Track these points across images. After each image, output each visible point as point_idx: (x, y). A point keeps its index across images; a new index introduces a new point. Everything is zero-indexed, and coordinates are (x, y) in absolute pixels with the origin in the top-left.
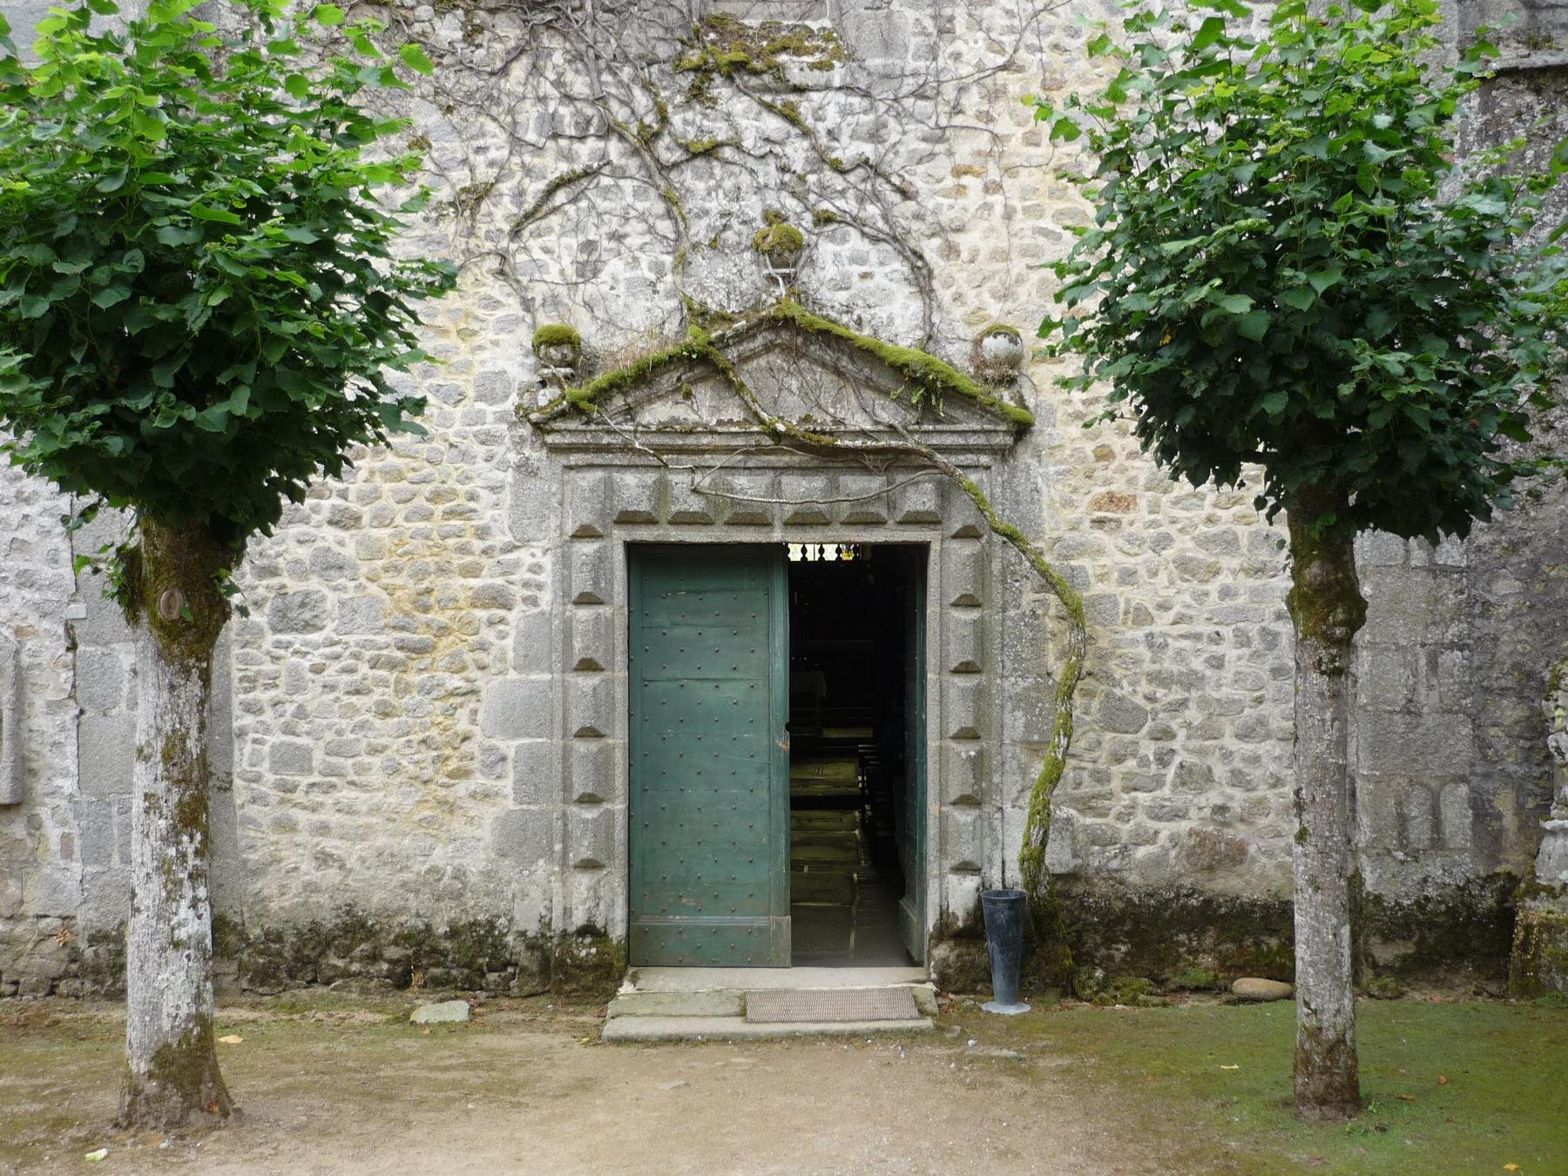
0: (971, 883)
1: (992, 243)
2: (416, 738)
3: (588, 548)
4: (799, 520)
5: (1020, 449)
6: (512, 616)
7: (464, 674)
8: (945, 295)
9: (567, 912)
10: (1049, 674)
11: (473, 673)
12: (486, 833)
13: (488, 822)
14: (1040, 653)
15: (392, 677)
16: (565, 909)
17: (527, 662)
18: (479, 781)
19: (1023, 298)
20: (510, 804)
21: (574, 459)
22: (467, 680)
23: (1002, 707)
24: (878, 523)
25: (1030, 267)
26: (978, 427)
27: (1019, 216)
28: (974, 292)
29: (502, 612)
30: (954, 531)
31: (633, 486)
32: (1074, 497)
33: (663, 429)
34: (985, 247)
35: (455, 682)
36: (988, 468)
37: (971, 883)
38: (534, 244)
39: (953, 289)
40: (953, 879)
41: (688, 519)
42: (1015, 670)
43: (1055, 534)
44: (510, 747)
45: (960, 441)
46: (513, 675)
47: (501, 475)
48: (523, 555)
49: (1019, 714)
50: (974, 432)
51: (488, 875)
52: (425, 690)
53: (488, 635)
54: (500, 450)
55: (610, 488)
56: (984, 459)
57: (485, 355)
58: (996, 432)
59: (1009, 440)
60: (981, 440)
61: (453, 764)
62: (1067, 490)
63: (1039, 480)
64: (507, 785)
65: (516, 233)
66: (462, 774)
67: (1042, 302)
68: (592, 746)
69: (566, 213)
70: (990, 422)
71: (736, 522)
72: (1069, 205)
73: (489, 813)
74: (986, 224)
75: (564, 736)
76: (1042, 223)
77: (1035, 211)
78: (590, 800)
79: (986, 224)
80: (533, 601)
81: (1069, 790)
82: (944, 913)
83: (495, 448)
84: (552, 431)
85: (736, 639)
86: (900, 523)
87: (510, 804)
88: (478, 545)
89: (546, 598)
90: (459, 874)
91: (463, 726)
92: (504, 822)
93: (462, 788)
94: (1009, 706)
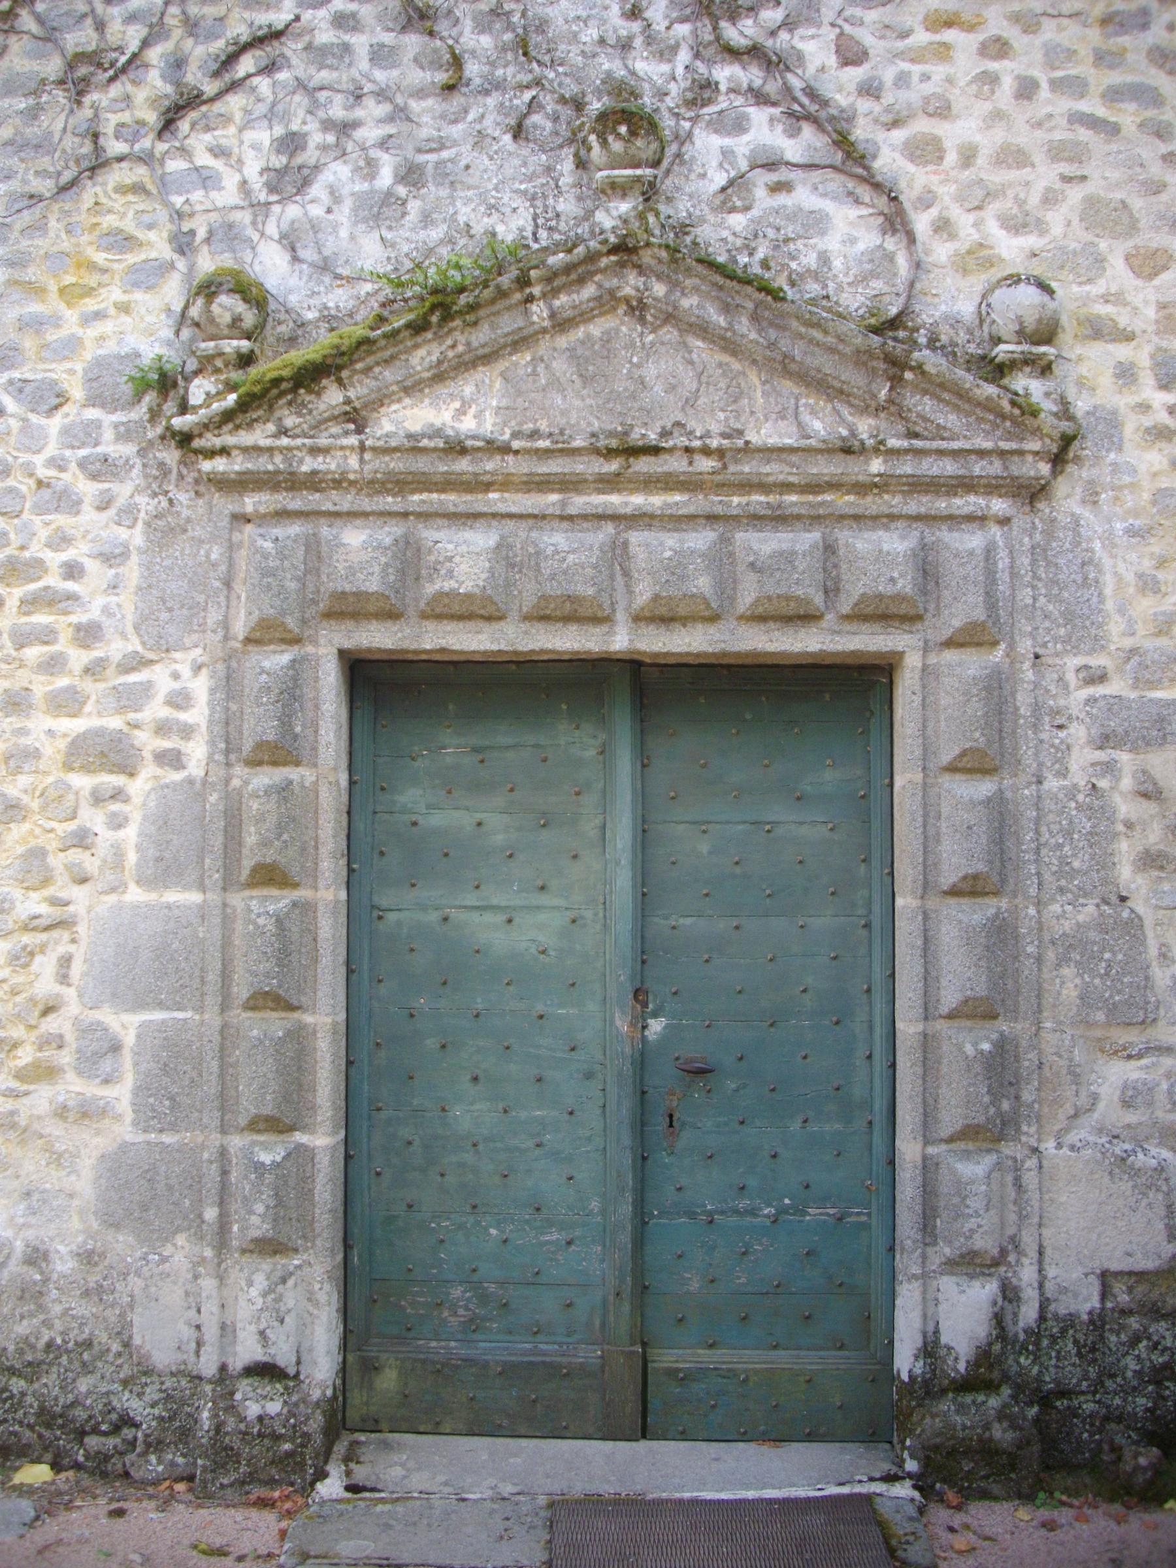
0: (983, 1292)
1: (999, 135)
3: (278, 659)
4: (663, 611)
5: (1061, 487)
6: (138, 786)
7: (46, 892)
8: (922, 223)
9: (227, 1330)
10: (1123, 899)
11: (63, 888)
13: (87, 1164)
14: (1105, 863)
16: (223, 1327)
18: (73, 1086)
19: (1057, 230)
20: (125, 1131)
21: (250, 503)
22: (54, 902)
23: (1039, 960)
24: (806, 617)
25: (1067, 179)
26: (988, 445)
27: (1044, 92)
28: (971, 218)
29: (117, 780)
30: (947, 633)
32: (1161, 575)
33: (413, 446)
34: (988, 142)
35: (33, 905)
36: (1004, 521)
37: (983, 1292)
38: (200, 142)
39: (934, 212)
40: (948, 1284)
41: (456, 608)
42: (1061, 890)
43: (1128, 643)
45: (949, 467)
46: (135, 894)
47: (123, 533)
48: (160, 677)
49: (1068, 971)
50: (982, 453)
51: (88, 1258)
53: (94, 819)
54: (123, 491)
56: (999, 506)
57: (107, 327)
58: (1021, 453)
59: (1045, 468)
60: (995, 467)
62: (1147, 564)
63: (1097, 545)
64: (121, 1095)
65: (168, 125)
66: (44, 1072)
67: (1089, 237)
68: (276, 1023)
69: (253, 89)
70: (1009, 436)
72: (1130, 78)
74: (987, 106)
75: (224, 1008)
76: (1084, 106)
77: (1074, 86)
79: (987, 106)
80: (172, 759)
81: (1159, 1114)
82: (930, 1349)
83: (115, 487)
84: (211, 454)
85: (545, 835)
86: (847, 618)
87: (125, 1131)
88: (79, 658)
89: (197, 752)
90: (37, 1257)
91: (45, 985)
93: (42, 1098)
94: (1051, 955)
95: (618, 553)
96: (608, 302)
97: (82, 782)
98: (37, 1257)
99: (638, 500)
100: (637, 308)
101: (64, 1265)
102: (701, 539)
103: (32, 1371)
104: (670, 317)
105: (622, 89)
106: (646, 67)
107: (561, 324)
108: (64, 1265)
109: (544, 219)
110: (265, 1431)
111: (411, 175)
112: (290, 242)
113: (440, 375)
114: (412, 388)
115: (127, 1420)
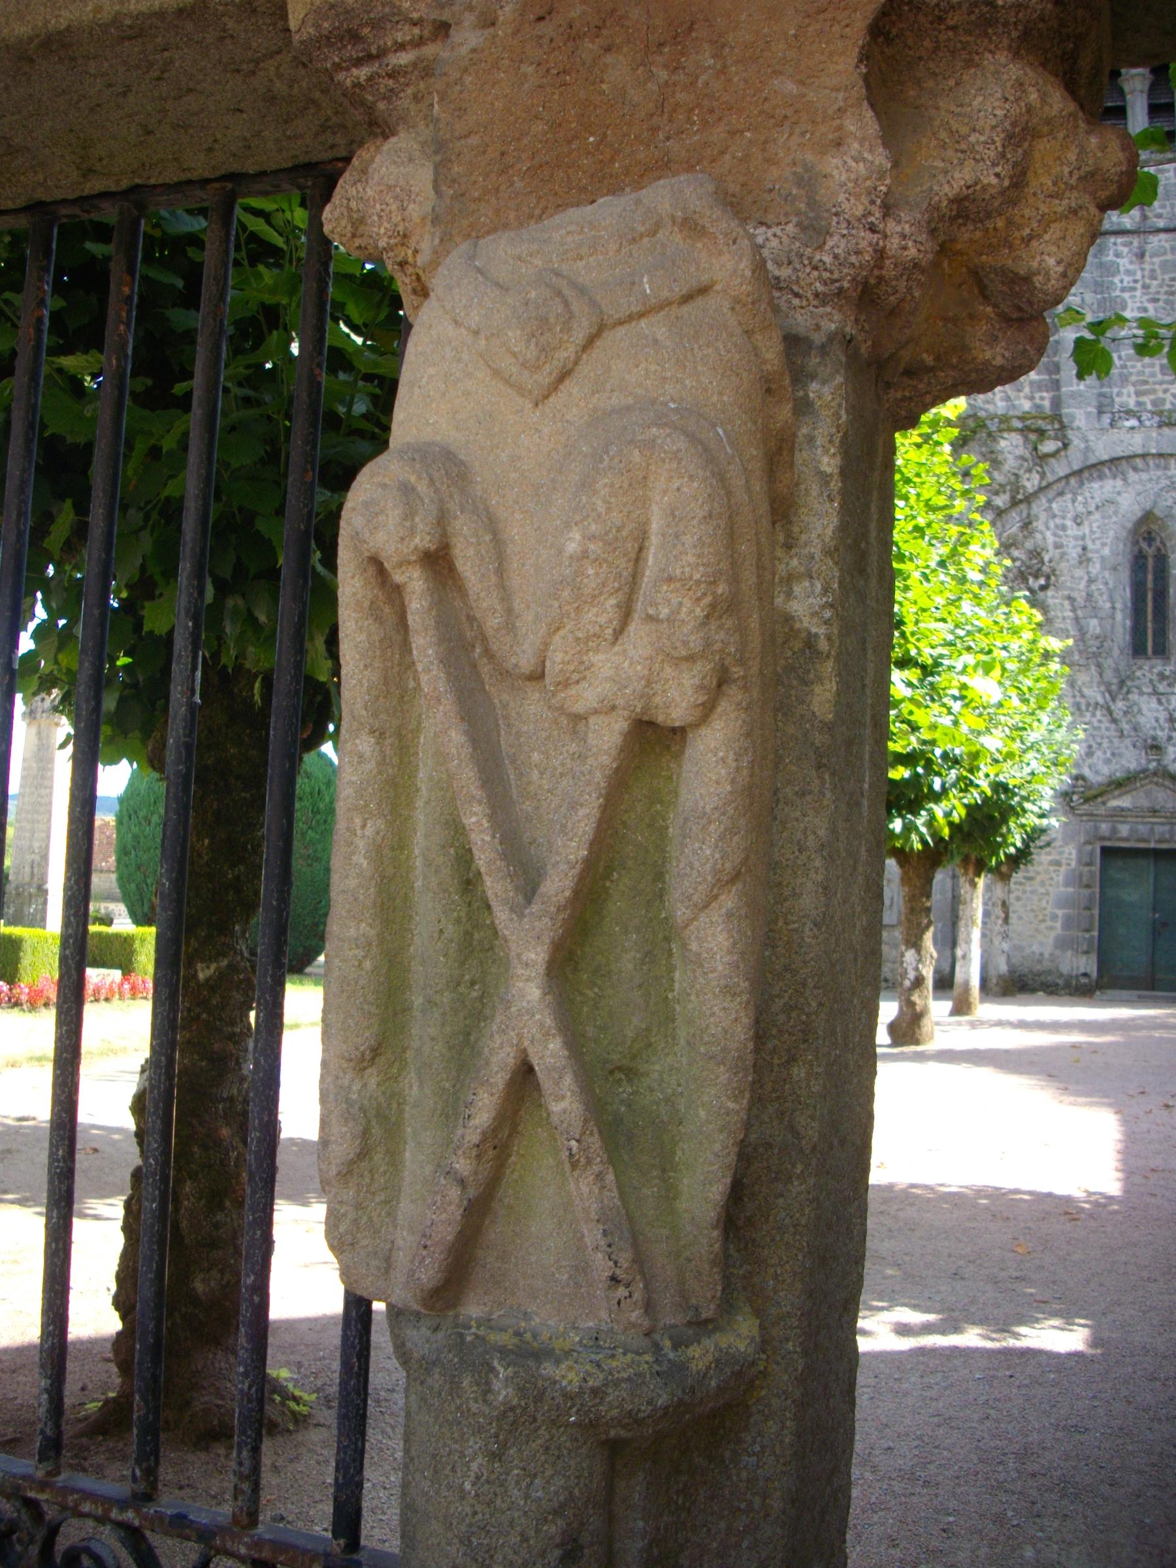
2: (1029, 908)
3: (1089, 848)
9: (1078, 968)
12: (1051, 941)
15: (1021, 888)
17: (1067, 884)
18: (1049, 923)
31: (1104, 827)
33: (1115, 809)
35: (1042, 890)
44: (1060, 913)
46: (1062, 889)
48: (1066, 850)
51: (1051, 955)
52: (1032, 892)
53: (1054, 875)
55: (1096, 828)
61: (1040, 918)
64: (1058, 925)
66: (1043, 921)
68: (1087, 913)
71: (1139, 840)
73: (1053, 934)
78: (1088, 931)
80: (1069, 865)
89: (1073, 864)
90: (1041, 954)
92: (1057, 938)
93: (1043, 926)
95: (1152, 830)
96: (1151, 782)
97: (1052, 868)
98: (1041, 954)
99: (1156, 820)
100: (1157, 784)
101: (1046, 955)
102: (1167, 828)
103: (1040, 975)
104: (1163, 785)
105: (1154, 738)
106: (1160, 733)
107: (1142, 786)
108: (1046, 955)
109: (1139, 764)
110: (1085, 985)
111: (1113, 754)
112: (1090, 767)
113: (1120, 795)
114: (1114, 798)
115: (1058, 985)
